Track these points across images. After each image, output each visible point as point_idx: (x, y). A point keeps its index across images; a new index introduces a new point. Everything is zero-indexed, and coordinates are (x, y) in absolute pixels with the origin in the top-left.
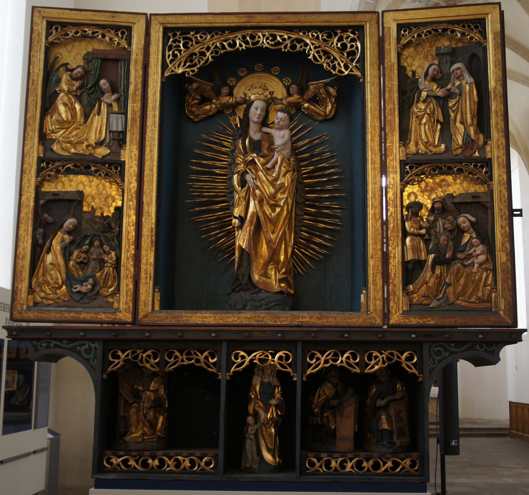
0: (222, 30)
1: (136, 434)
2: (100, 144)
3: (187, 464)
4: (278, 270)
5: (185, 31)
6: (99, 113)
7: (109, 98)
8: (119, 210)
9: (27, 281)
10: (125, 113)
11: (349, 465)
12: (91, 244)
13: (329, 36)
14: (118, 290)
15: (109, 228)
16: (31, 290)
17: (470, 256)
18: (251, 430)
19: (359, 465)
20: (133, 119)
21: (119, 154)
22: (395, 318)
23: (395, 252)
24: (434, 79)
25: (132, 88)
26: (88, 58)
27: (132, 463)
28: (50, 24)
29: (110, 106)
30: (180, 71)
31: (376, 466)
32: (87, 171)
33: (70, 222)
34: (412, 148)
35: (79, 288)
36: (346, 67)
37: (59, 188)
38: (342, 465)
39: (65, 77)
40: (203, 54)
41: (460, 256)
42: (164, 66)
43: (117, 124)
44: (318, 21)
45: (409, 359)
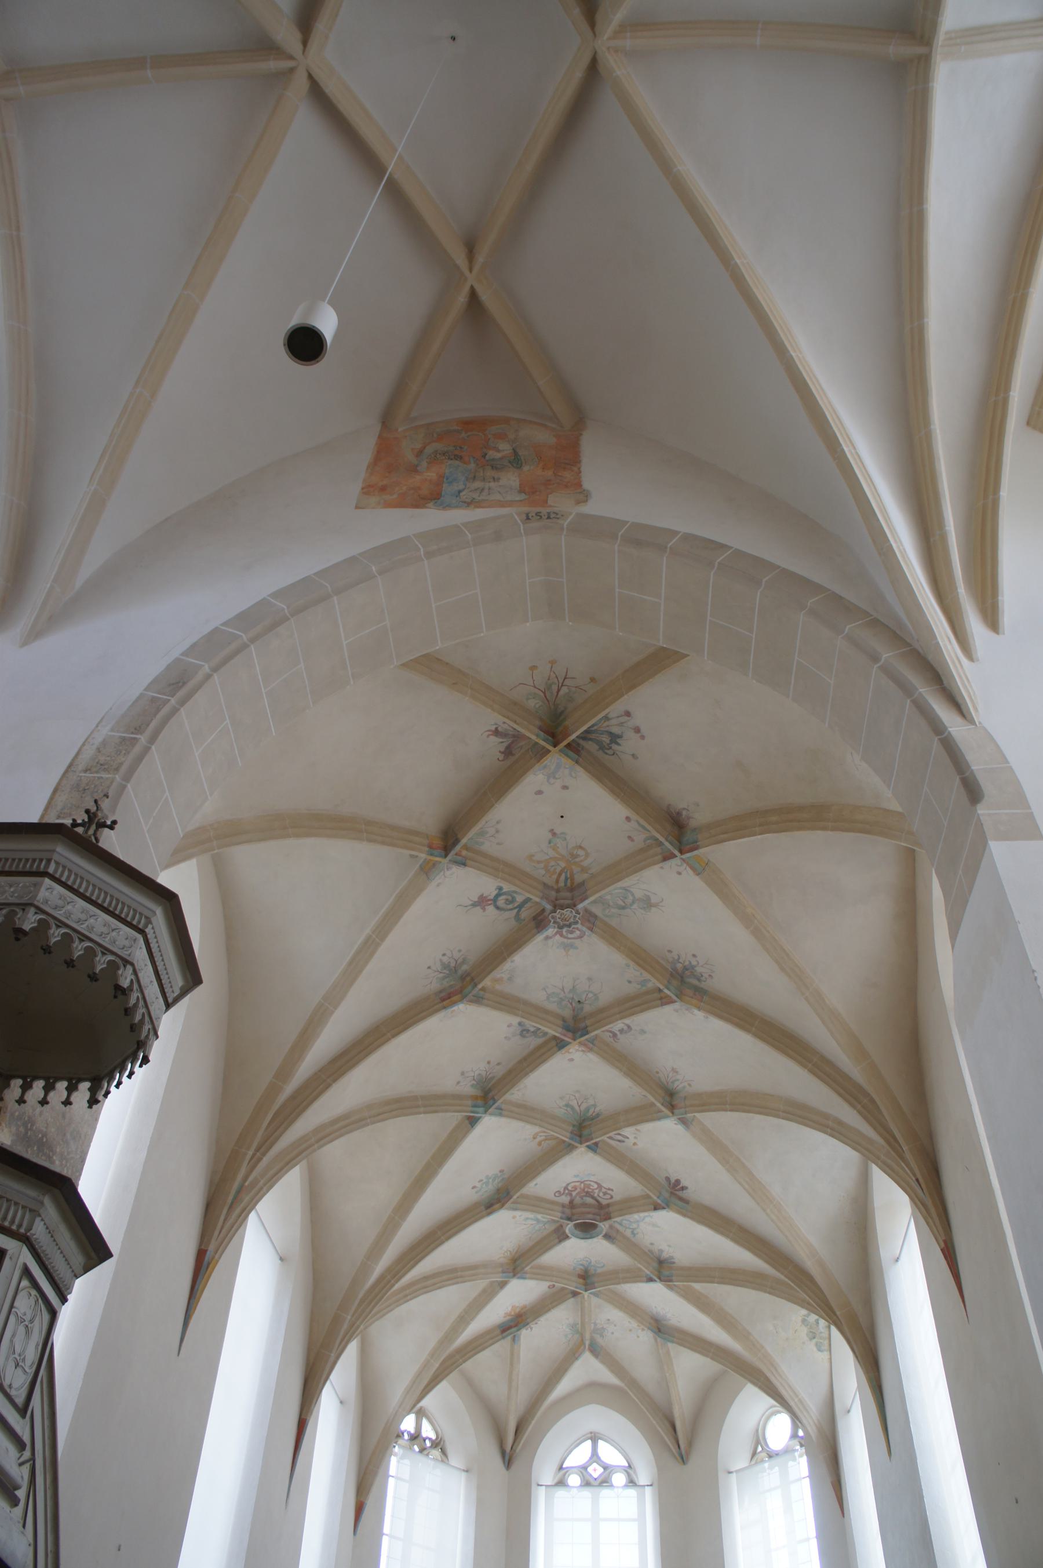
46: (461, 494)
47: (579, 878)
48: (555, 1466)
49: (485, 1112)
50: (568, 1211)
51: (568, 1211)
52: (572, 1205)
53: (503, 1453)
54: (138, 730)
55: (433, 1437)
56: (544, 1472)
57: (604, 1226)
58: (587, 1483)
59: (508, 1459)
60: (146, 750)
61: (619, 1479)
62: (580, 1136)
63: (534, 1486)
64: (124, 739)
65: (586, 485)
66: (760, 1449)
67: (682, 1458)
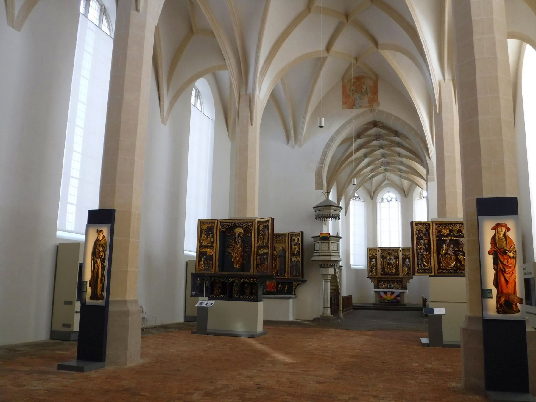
0: (230, 222)
1: (216, 292)
2: (209, 243)
3: (222, 296)
4: (239, 265)
5: (224, 223)
6: (209, 237)
7: (211, 235)
8: (213, 254)
9: (197, 267)
10: (214, 238)
11: (247, 297)
12: (208, 260)
13: (247, 223)
14: (212, 268)
15: (211, 258)
16: (198, 268)
17: (265, 263)
18: (234, 292)
19: (248, 297)
20: (215, 239)
21: (212, 245)
22: (255, 273)
23: (255, 262)
24: (263, 231)
25: (215, 233)
26: (207, 227)
27: (214, 296)
28: (201, 222)
29: (211, 236)
30: (222, 230)
31: (251, 298)
32: (207, 248)
33: (205, 257)
34: (258, 244)
35: (206, 268)
36: (250, 229)
37: (203, 251)
38: (246, 297)
39: (204, 231)
40: (226, 227)
41: (264, 263)
42: (220, 229)
43: (212, 240)
44: (245, 221)
45: (256, 280)
46: (359, 104)
47: (380, 134)
48: (381, 198)
49: (366, 158)
50: (381, 164)
51: (381, 164)
52: (382, 163)
53: (371, 198)
54: (323, 165)
55: (357, 196)
56: (379, 199)
57: (388, 166)
58: (388, 201)
59: (372, 198)
60: (324, 167)
61: (394, 200)
62: (383, 157)
63: (377, 203)
64: (321, 166)
65: (380, 100)
66: (421, 195)
67: (406, 197)
